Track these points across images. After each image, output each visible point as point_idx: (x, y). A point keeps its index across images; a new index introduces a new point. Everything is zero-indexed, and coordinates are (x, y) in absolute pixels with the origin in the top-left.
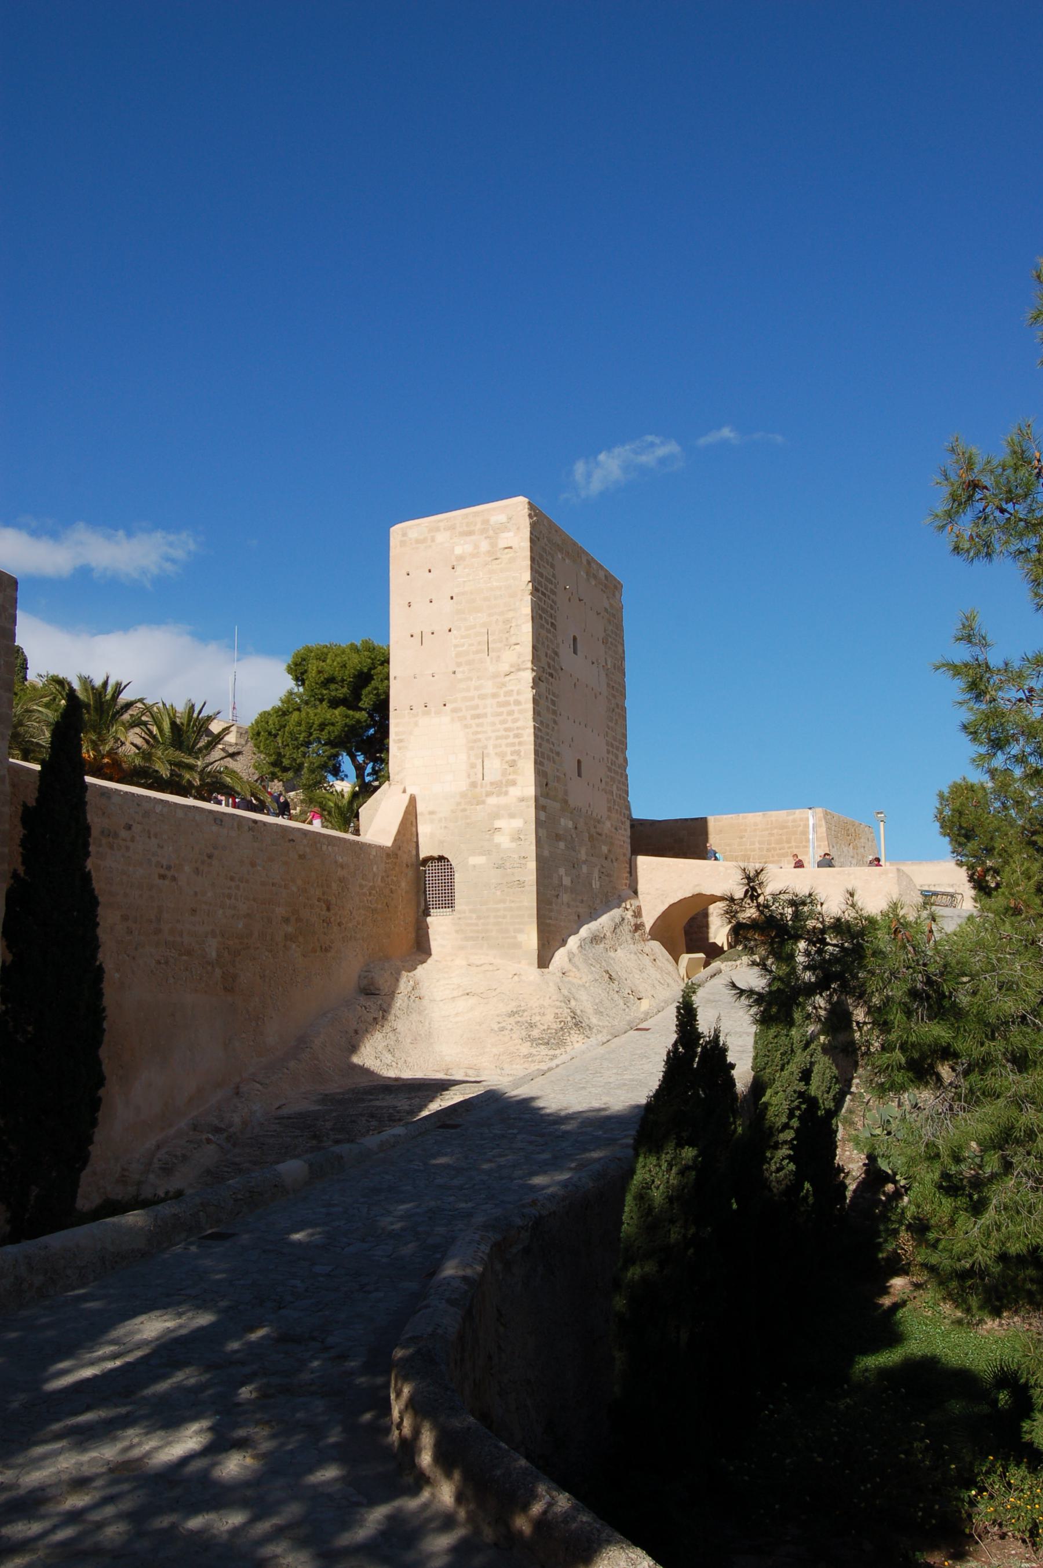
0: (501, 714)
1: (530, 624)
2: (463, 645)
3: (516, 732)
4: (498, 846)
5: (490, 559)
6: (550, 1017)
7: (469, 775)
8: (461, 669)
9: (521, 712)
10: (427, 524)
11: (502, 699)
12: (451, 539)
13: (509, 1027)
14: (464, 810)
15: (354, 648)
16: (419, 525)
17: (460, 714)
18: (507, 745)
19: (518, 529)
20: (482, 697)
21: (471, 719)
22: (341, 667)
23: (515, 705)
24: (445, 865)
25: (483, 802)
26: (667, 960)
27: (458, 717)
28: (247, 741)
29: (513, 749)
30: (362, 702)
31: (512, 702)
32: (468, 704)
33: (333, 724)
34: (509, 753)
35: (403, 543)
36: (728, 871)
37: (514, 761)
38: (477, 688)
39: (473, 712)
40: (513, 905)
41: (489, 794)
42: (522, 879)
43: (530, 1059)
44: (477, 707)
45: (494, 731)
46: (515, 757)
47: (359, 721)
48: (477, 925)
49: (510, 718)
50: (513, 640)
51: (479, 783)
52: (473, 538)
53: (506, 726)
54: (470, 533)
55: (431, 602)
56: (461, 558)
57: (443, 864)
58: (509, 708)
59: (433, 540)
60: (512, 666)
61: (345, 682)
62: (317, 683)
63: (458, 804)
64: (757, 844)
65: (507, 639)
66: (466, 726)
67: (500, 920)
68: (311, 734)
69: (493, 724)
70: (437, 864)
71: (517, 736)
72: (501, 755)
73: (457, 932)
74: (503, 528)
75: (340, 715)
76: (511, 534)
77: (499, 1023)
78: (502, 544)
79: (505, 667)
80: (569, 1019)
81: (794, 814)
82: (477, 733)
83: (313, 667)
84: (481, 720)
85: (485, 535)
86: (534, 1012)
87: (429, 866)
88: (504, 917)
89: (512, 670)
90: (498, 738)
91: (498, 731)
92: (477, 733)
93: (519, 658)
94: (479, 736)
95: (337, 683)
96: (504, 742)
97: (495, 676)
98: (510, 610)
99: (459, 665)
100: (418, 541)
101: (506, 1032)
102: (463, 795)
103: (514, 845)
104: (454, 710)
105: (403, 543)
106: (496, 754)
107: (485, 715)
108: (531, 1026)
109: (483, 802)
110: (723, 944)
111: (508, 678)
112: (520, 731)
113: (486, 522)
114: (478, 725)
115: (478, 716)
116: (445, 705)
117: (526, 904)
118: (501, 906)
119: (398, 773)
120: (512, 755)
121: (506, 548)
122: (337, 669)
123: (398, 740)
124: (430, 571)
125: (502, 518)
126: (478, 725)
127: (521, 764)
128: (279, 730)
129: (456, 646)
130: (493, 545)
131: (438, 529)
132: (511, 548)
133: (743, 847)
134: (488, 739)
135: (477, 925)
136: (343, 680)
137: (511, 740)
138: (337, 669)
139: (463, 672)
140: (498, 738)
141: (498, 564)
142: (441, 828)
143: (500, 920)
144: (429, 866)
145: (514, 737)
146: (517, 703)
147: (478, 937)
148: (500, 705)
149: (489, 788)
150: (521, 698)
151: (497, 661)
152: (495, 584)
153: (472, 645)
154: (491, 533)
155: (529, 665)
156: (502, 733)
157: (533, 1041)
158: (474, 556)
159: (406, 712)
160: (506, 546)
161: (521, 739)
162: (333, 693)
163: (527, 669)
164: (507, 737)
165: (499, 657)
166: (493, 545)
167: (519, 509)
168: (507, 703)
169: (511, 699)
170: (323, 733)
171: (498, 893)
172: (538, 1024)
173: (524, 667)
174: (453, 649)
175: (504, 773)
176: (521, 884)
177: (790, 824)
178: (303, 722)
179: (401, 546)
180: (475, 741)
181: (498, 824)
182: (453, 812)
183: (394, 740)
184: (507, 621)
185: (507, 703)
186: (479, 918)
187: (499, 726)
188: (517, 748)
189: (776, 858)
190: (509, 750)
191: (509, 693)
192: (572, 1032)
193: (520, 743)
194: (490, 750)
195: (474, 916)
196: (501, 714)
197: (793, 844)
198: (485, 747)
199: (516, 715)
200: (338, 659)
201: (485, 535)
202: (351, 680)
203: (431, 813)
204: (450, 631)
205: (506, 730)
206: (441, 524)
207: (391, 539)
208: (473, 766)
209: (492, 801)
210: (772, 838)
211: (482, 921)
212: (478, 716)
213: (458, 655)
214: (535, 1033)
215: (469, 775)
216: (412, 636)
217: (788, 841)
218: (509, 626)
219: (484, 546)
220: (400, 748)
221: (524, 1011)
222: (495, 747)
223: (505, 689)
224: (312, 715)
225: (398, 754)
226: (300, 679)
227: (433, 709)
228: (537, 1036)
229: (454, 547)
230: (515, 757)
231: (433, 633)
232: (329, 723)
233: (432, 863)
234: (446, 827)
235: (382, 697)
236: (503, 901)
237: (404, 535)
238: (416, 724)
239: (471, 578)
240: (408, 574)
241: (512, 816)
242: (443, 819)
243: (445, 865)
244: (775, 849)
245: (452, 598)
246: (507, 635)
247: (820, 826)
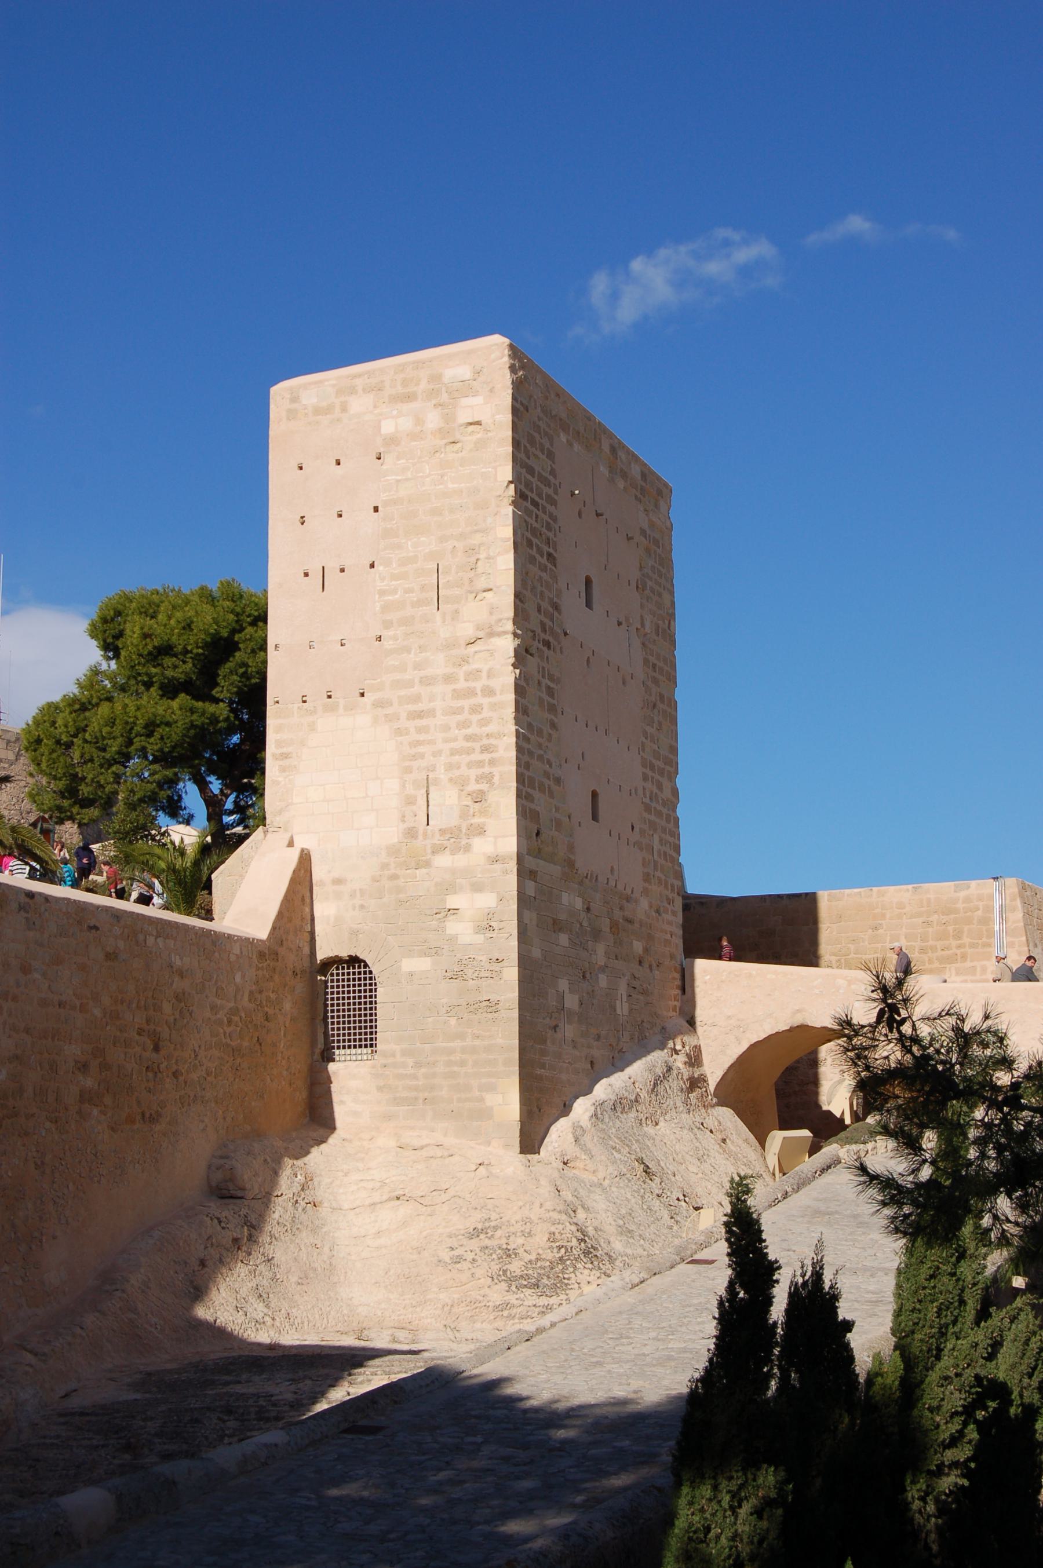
0: (459, 711)
1: (510, 557)
2: (395, 591)
3: (485, 741)
4: (452, 939)
5: (444, 441)
6: (540, 1240)
7: (404, 817)
8: (391, 633)
9: (493, 707)
10: (334, 382)
11: (462, 684)
12: (375, 407)
13: (470, 1256)
14: (394, 877)
15: (207, 596)
16: (321, 382)
17: (389, 711)
18: (470, 765)
19: (491, 390)
20: (427, 681)
21: (408, 719)
22: (184, 628)
23: (484, 696)
24: (359, 973)
25: (428, 864)
26: (746, 1141)
27: (386, 716)
28: (18, 756)
29: (480, 771)
30: (218, 689)
32: (402, 693)
33: (168, 724)
34: (473, 778)
35: (292, 414)
36: (853, 987)
37: (482, 792)
38: (417, 666)
39: (411, 707)
40: (477, 1042)
41: (437, 850)
42: (494, 998)
43: (505, 1313)
44: (417, 699)
45: (446, 741)
46: (484, 787)
47: (214, 720)
48: (414, 1077)
49: (475, 718)
50: (482, 583)
51: (421, 832)
53: (469, 731)
54: (409, 397)
55: (340, 516)
56: (392, 441)
57: (357, 970)
58: (472, 701)
59: (344, 409)
60: (478, 628)
61: (189, 655)
62: (141, 655)
63: (385, 866)
64: (903, 938)
65: (471, 581)
66: (399, 732)
67: (456, 1069)
68: (130, 742)
69: (446, 728)
70: (346, 971)
71: (485, 749)
72: (461, 783)
73: (380, 1089)
74: (465, 389)
75: (181, 709)
76: (479, 400)
77: (452, 1249)
78: (464, 417)
79: (468, 630)
80: (574, 1242)
81: (969, 887)
82: (419, 743)
83: (133, 629)
84: (424, 722)
85: (434, 402)
86: (512, 1229)
87: (332, 975)
88: (462, 1063)
89: (480, 634)
90: (454, 752)
91: (455, 740)
92: (419, 743)
93: (491, 614)
94: (421, 749)
95: (175, 655)
96: (465, 759)
98: (477, 531)
99: (388, 625)
100: (318, 411)
101: (465, 1265)
102: (393, 851)
103: (480, 938)
104: (379, 704)
105: (292, 414)
106: (451, 780)
107: (431, 713)
108: (509, 1254)
109: (428, 864)
110: (843, 1113)
111: (472, 649)
112: (493, 741)
113: (436, 378)
114: (420, 730)
115: (420, 715)
116: (362, 695)
117: (500, 1041)
118: (457, 1044)
119: (280, 812)
120: (477, 781)
121: (471, 424)
122: (176, 631)
123: (282, 754)
124: (338, 463)
125: (464, 372)
126: (420, 730)
127: (493, 797)
128: (75, 736)
129: (382, 593)
130: (449, 418)
131: (352, 391)
132: (478, 423)
133: (879, 945)
134: (437, 754)
135: (414, 1077)
136: (186, 652)
137: (477, 756)
138: (176, 631)
140: (454, 752)
141: (457, 452)
142: (354, 909)
143: (456, 1069)
144: (332, 975)
145: (482, 752)
146: (489, 692)
147: (416, 1099)
148: (457, 695)
149: (437, 840)
150: (496, 683)
151: (453, 619)
152: (450, 486)
154: (445, 397)
155: (509, 626)
157: (510, 1281)
158: (413, 436)
159: (296, 706)
160: (470, 421)
161: (494, 755)
162: (169, 673)
163: (505, 633)
164: (469, 751)
165: (457, 611)
166: (449, 418)
167: (493, 356)
168: (471, 693)
169: (478, 685)
170: (152, 740)
171: (453, 1021)
172: (521, 1251)
173: (500, 629)
174: (377, 596)
175: (464, 814)
176: (492, 1006)
177: (960, 905)
178: (118, 721)
179: (289, 419)
180: (414, 757)
181: (452, 902)
182: (375, 880)
183: (274, 755)
184: (470, 550)
185: (471, 693)
186: (418, 1065)
187: (457, 731)
188: (487, 770)
189: (936, 965)
190: (473, 773)
192: (579, 1265)
193: (492, 762)
194: (441, 774)
195: (410, 1061)
196: (459, 711)
197: (966, 940)
198: (433, 768)
199: (486, 713)
200: (179, 615)
202: (200, 651)
203: (338, 881)
204: (372, 566)
205: (468, 738)
206: (358, 382)
207: (272, 406)
208: (410, 801)
209: (443, 861)
210: (930, 929)
211: (423, 1070)
212: (420, 715)
213: (386, 608)
214: (516, 1267)
215: (404, 817)
216: (306, 575)
217: (958, 936)
218: (473, 560)
219: (433, 420)
220: (283, 769)
221: (496, 1228)
222: (450, 767)
224: (132, 709)
225: (280, 779)
226: (111, 646)
227: (342, 702)
228: (518, 1273)
229: (380, 421)
230: (484, 787)
231: (342, 570)
232: (161, 723)
233: (337, 968)
234: (362, 907)
235: (253, 681)
236: (462, 1036)
237: (295, 399)
238: (312, 727)
239: (409, 475)
240: (301, 468)
241: (477, 888)
242: (358, 894)
243: (359, 973)
244: (933, 949)
245: (376, 509)
246: (472, 574)
247: (1014, 909)
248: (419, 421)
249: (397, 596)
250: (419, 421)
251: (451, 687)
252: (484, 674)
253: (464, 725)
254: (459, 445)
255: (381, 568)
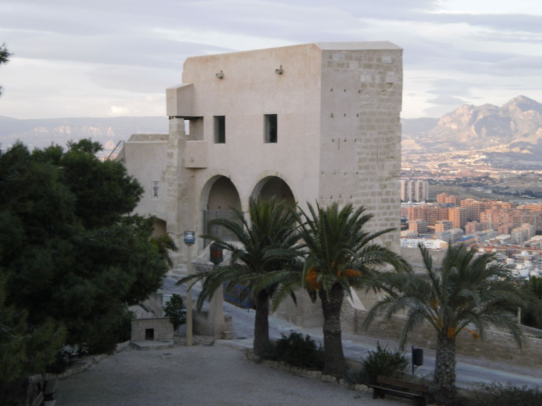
2: (362, 154)
3: (391, 222)
8: (361, 172)
10: (345, 52)
11: (384, 197)
20: (373, 194)
31: (389, 200)
38: (370, 187)
46: (390, 240)
49: (388, 211)
50: (391, 155)
52: (372, 70)
54: (369, 66)
56: (364, 85)
60: (390, 173)
65: (388, 153)
78: (388, 80)
79: (386, 174)
89: (391, 176)
97: (381, 179)
99: (360, 168)
111: (388, 182)
113: (379, 60)
129: (359, 153)
130: (383, 79)
131: (351, 59)
139: (363, 174)
153: (367, 154)
156: (384, 222)
166: (383, 79)
187: (382, 216)
191: (388, 193)
199: (392, 210)
201: (378, 71)
213: (360, 160)
223: (385, 190)
230: (390, 240)
248: (373, 79)
249: (364, 156)
250: (373, 79)
251: (380, 198)
252: (391, 193)
253: (385, 214)
254: (385, 92)
255: (359, 142)
